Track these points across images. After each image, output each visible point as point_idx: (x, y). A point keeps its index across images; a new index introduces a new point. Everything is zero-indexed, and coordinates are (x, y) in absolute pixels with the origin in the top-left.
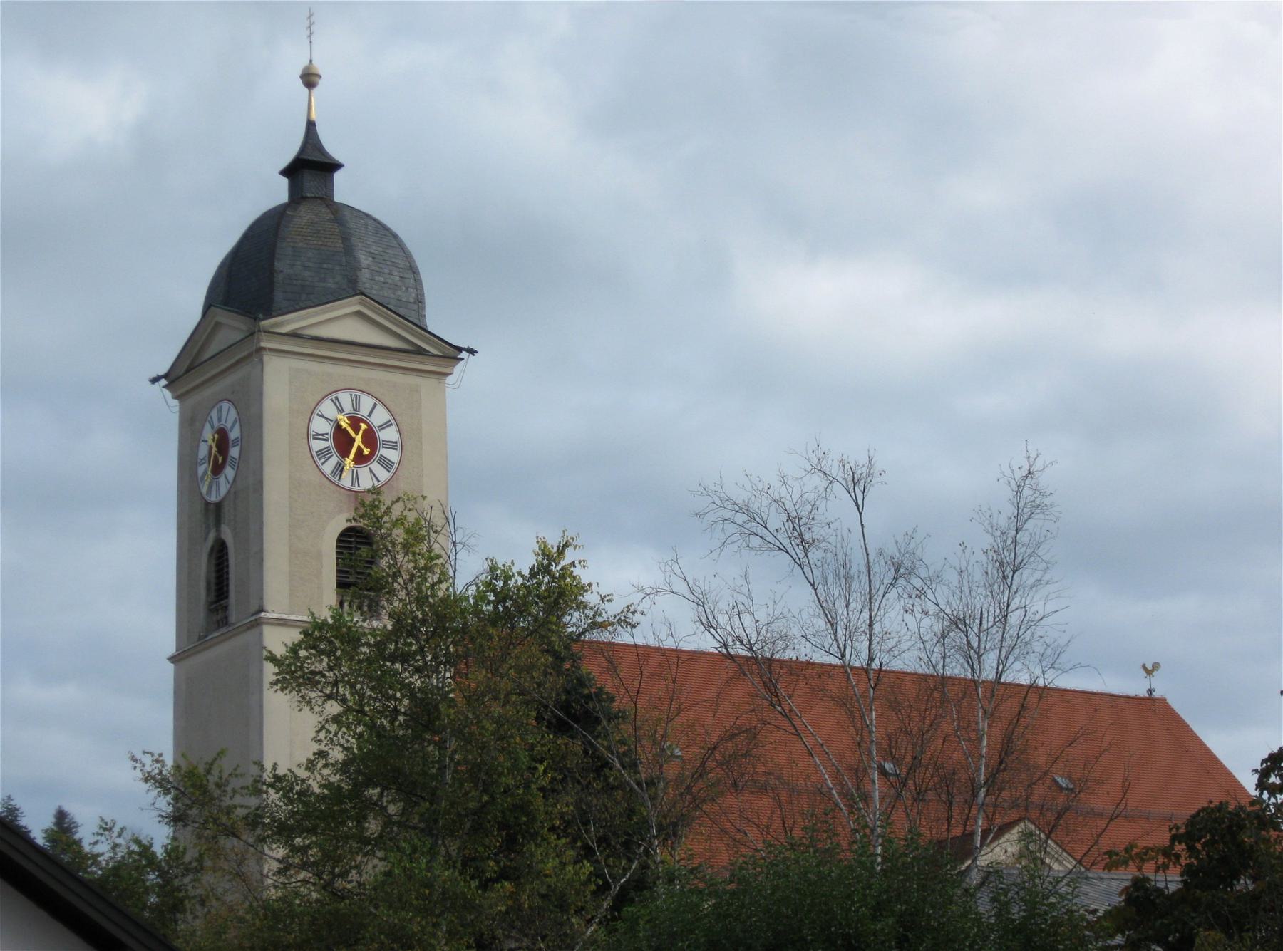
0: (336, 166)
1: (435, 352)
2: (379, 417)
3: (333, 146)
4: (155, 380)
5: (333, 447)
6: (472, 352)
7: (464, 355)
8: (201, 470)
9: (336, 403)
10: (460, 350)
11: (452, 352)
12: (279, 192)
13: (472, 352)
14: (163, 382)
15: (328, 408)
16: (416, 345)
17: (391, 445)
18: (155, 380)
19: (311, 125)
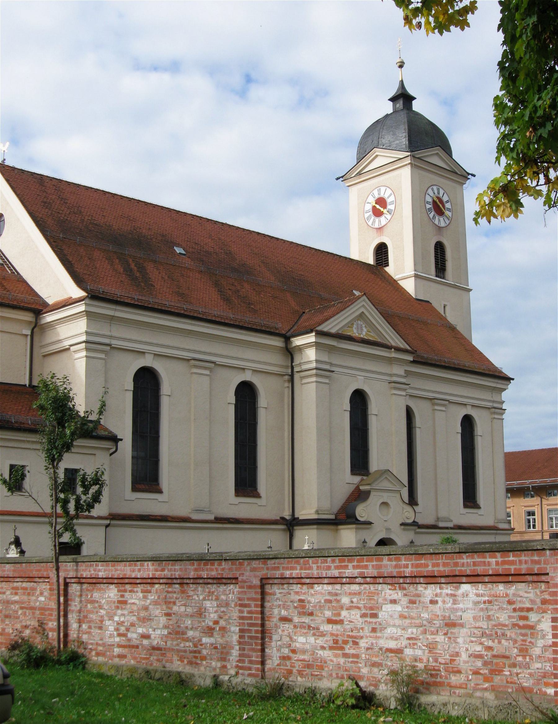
0: (414, 98)
1: (459, 173)
2: (445, 199)
3: (411, 91)
4: (337, 179)
5: (432, 208)
6: (474, 176)
7: (470, 177)
8: (367, 215)
9: (433, 190)
10: (469, 174)
11: (466, 175)
12: (389, 108)
13: (474, 176)
14: (341, 179)
15: (430, 192)
16: (455, 170)
17: (449, 210)
18: (337, 179)
19: (402, 82)
